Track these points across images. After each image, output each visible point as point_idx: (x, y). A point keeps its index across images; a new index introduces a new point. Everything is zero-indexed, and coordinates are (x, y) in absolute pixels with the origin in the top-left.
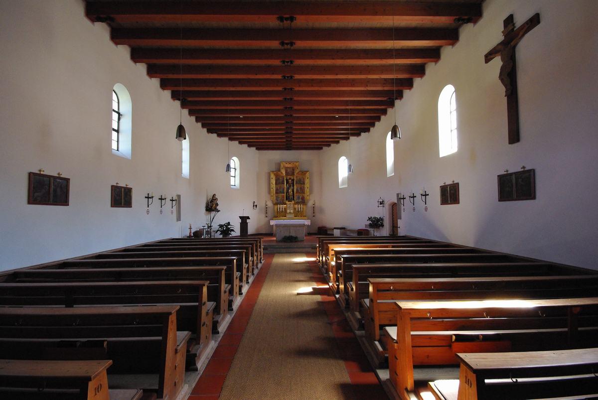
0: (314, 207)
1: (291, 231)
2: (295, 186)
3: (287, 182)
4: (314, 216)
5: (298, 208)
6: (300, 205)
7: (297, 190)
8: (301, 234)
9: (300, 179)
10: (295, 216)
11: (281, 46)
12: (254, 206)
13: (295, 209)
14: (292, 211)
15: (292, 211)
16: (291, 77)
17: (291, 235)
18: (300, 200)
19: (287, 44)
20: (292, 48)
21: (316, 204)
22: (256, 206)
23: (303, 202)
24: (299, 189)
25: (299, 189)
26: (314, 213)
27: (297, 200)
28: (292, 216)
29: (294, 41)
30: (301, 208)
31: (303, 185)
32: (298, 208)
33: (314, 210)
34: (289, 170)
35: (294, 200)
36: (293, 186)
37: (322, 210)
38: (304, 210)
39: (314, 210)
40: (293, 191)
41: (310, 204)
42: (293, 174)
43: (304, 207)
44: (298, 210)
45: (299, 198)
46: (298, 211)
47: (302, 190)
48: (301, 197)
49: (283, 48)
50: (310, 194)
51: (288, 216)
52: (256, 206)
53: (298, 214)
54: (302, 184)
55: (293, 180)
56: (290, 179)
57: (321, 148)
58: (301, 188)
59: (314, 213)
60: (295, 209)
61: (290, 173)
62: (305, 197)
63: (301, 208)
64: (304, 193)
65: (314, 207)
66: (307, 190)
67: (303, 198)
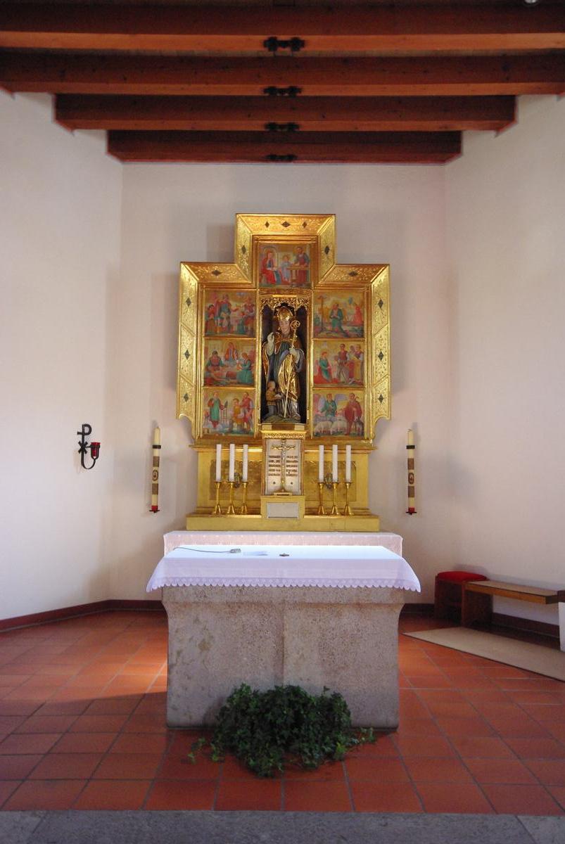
0: (411, 464)
1: (294, 643)
2: (311, 349)
3: (271, 323)
4: (411, 511)
5: (327, 464)
6: (341, 450)
7: (323, 369)
8: (370, 671)
9: (336, 306)
10: (311, 512)
11: (266, 49)
12: (83, 451)
13: (310, 469)
14: (292, 482)
15: (292, 482)
16: (293, 90)
17: (291, 678)
18: (340, 423)
19: (284, 44)
20: (298, 54)
21: (423, 446)
22: (95, 448)
23: (354, 427)
24: (333, 363)
25: (333, 363)
26: (411, 493)
27: (321, 425)
28: (295, 508)
29: (299, 86)
30: (342, 465)
31: (350, 344)
32: (327, 464)
33: (411, 480)
34: (278, 262)
35: (303, 420)
36: (303, 345)
37: (455, 480)
38: (362, 473)
39: (411, 480)
40: (301, 376)
41: (391, 444)
42: (303, 279)
43: (362, 460)
44: (328, 475)
45: (331, 411)
46: (328, 484)
47: (351, 372)
48: (341, 406)
49: (271, 54)
50: (393, 390)
51: (271, 507)
52: (95, 448)
53: (329, 503)
54: (347, 335)
55: (301, 315)
56: (285, 307)
57: (443, 147)
58: (343, 357)
59: (411, 493)
60: (310, 469)
61: (286, 275)
62: (365, 408)
63: (342, 465)
64: (360, 385)
65: (411, 464)
66: (379, 373)
67: (354, 413)
